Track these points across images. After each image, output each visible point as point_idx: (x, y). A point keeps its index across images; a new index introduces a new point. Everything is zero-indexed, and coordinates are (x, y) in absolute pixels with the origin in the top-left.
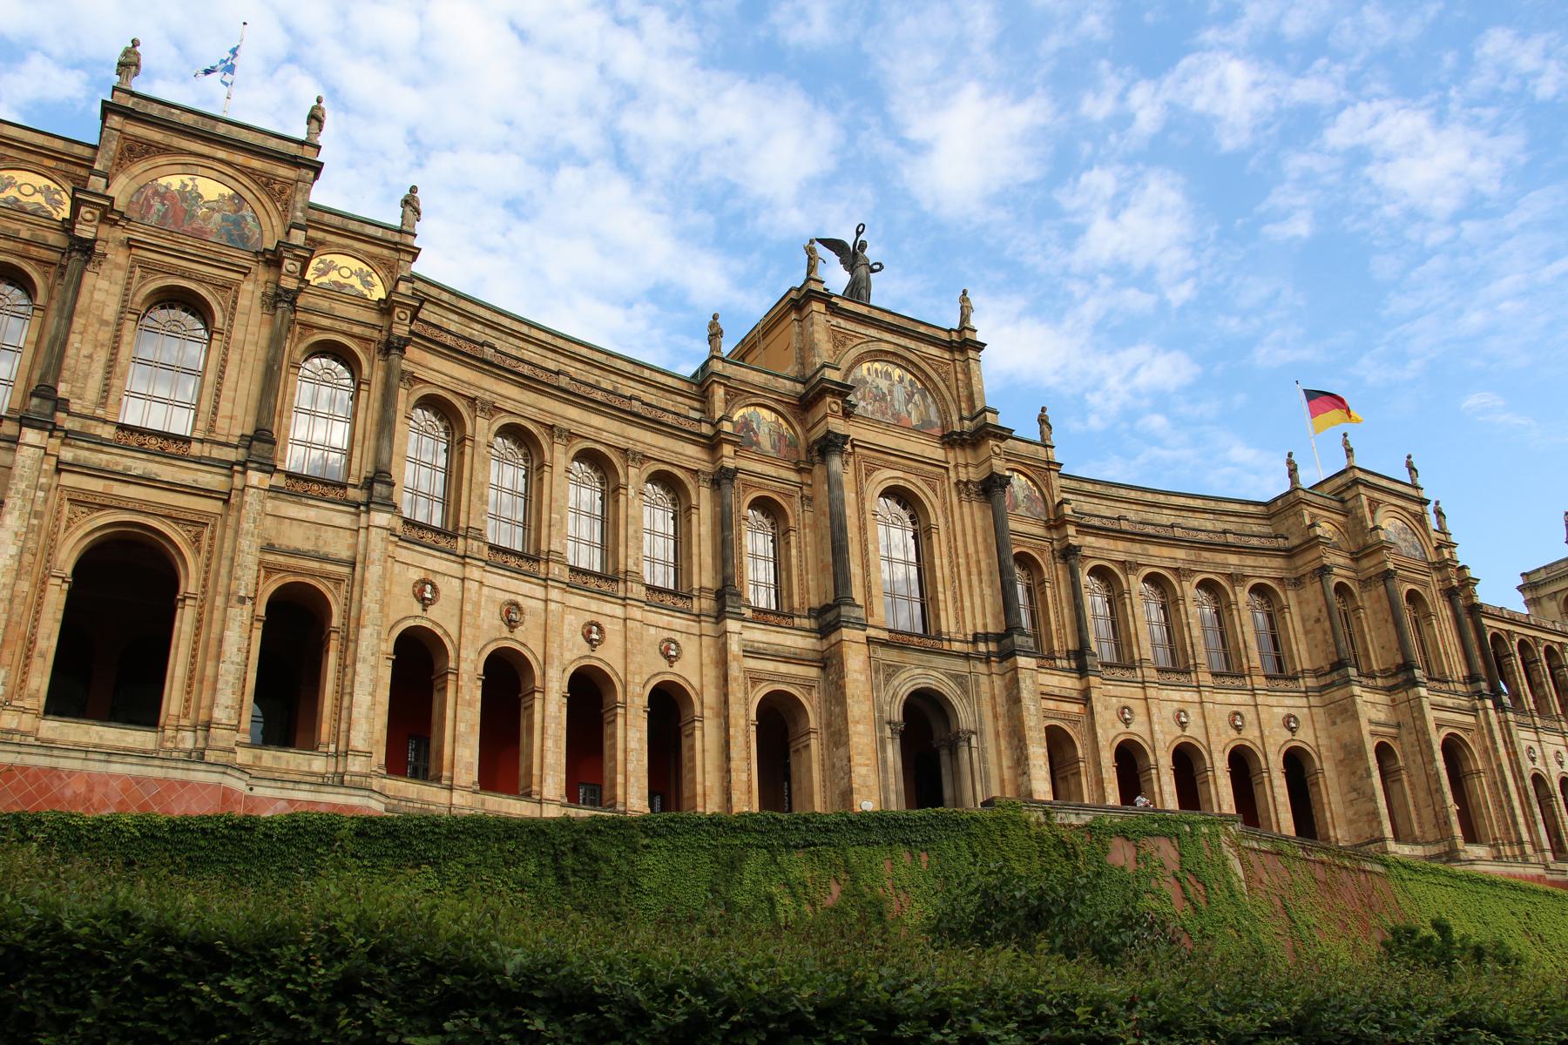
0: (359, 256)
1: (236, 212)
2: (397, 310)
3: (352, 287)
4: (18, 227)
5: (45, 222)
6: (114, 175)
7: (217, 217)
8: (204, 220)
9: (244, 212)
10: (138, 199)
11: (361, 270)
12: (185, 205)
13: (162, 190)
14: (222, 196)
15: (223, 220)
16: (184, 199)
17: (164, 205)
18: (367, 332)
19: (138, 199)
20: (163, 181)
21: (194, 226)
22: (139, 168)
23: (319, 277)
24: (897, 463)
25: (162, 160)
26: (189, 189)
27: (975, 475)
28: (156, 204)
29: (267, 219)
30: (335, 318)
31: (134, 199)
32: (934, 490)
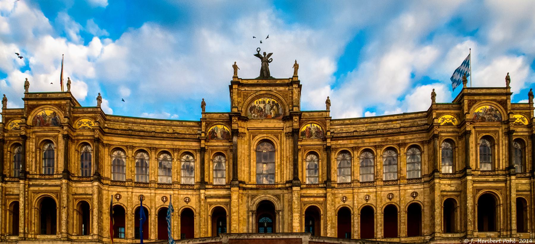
24: (264, 132)
27: (289, 130)
32: (277, 137)
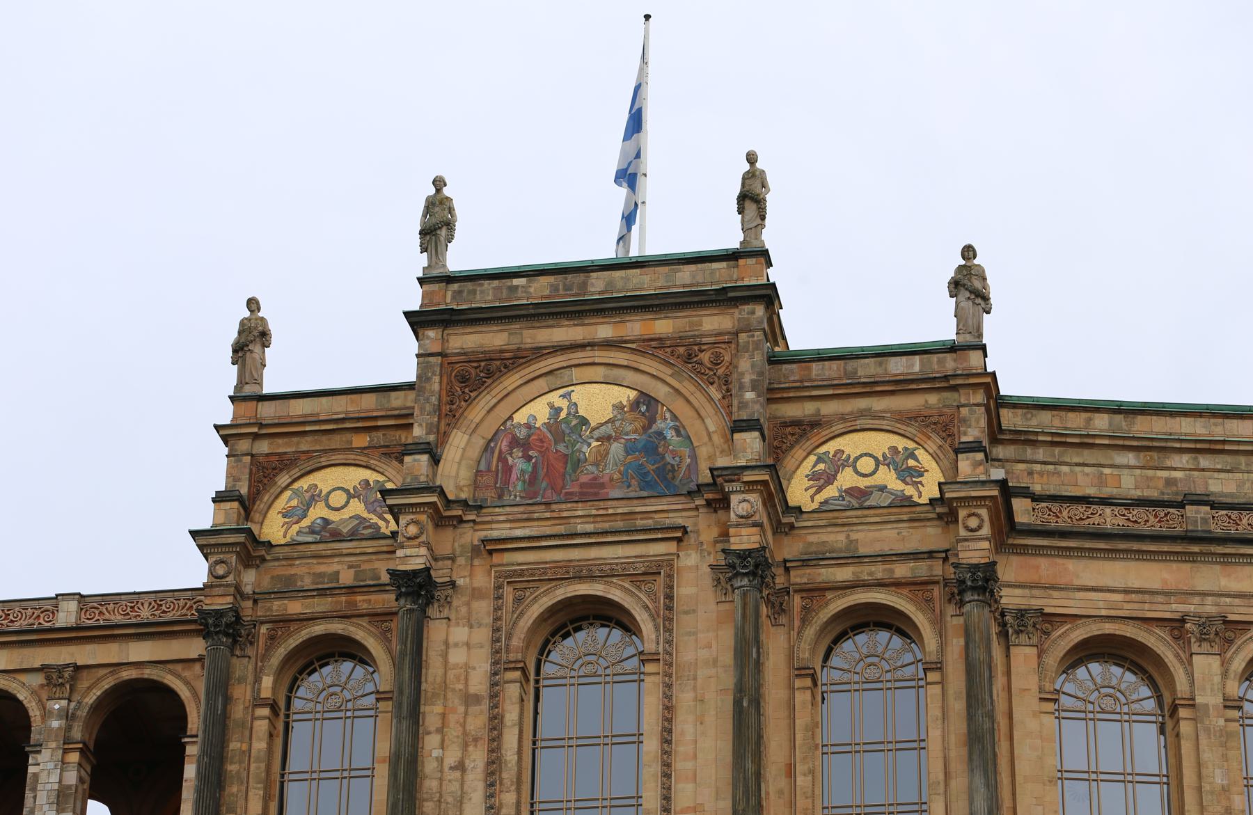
0: (885, 424)
1: (645, 428)
2: (962, 513)
3: (882, 489)
4: (336, 567)
5: (369, 546)
6: (443, 437)
7: (616, 448)
8: (597, 464)
9: (659, 424)
10: (489, 464)
11: (894, 450)
12: (561, 447)
13: (521, 434)
14: (619, 407)
15: (627, 453)
16: (559, 436)
17: (529, 458)
18: (921, 569)
19: (489, 464)
20: (521, 417)
21: (584, 479)
22: (476, 412)
23: (818, 492)
25: (512, 380)
26: (563, 415)
28: (518, 463)
29: (698, 422)
30: (859, 559)
31: (483, 467)
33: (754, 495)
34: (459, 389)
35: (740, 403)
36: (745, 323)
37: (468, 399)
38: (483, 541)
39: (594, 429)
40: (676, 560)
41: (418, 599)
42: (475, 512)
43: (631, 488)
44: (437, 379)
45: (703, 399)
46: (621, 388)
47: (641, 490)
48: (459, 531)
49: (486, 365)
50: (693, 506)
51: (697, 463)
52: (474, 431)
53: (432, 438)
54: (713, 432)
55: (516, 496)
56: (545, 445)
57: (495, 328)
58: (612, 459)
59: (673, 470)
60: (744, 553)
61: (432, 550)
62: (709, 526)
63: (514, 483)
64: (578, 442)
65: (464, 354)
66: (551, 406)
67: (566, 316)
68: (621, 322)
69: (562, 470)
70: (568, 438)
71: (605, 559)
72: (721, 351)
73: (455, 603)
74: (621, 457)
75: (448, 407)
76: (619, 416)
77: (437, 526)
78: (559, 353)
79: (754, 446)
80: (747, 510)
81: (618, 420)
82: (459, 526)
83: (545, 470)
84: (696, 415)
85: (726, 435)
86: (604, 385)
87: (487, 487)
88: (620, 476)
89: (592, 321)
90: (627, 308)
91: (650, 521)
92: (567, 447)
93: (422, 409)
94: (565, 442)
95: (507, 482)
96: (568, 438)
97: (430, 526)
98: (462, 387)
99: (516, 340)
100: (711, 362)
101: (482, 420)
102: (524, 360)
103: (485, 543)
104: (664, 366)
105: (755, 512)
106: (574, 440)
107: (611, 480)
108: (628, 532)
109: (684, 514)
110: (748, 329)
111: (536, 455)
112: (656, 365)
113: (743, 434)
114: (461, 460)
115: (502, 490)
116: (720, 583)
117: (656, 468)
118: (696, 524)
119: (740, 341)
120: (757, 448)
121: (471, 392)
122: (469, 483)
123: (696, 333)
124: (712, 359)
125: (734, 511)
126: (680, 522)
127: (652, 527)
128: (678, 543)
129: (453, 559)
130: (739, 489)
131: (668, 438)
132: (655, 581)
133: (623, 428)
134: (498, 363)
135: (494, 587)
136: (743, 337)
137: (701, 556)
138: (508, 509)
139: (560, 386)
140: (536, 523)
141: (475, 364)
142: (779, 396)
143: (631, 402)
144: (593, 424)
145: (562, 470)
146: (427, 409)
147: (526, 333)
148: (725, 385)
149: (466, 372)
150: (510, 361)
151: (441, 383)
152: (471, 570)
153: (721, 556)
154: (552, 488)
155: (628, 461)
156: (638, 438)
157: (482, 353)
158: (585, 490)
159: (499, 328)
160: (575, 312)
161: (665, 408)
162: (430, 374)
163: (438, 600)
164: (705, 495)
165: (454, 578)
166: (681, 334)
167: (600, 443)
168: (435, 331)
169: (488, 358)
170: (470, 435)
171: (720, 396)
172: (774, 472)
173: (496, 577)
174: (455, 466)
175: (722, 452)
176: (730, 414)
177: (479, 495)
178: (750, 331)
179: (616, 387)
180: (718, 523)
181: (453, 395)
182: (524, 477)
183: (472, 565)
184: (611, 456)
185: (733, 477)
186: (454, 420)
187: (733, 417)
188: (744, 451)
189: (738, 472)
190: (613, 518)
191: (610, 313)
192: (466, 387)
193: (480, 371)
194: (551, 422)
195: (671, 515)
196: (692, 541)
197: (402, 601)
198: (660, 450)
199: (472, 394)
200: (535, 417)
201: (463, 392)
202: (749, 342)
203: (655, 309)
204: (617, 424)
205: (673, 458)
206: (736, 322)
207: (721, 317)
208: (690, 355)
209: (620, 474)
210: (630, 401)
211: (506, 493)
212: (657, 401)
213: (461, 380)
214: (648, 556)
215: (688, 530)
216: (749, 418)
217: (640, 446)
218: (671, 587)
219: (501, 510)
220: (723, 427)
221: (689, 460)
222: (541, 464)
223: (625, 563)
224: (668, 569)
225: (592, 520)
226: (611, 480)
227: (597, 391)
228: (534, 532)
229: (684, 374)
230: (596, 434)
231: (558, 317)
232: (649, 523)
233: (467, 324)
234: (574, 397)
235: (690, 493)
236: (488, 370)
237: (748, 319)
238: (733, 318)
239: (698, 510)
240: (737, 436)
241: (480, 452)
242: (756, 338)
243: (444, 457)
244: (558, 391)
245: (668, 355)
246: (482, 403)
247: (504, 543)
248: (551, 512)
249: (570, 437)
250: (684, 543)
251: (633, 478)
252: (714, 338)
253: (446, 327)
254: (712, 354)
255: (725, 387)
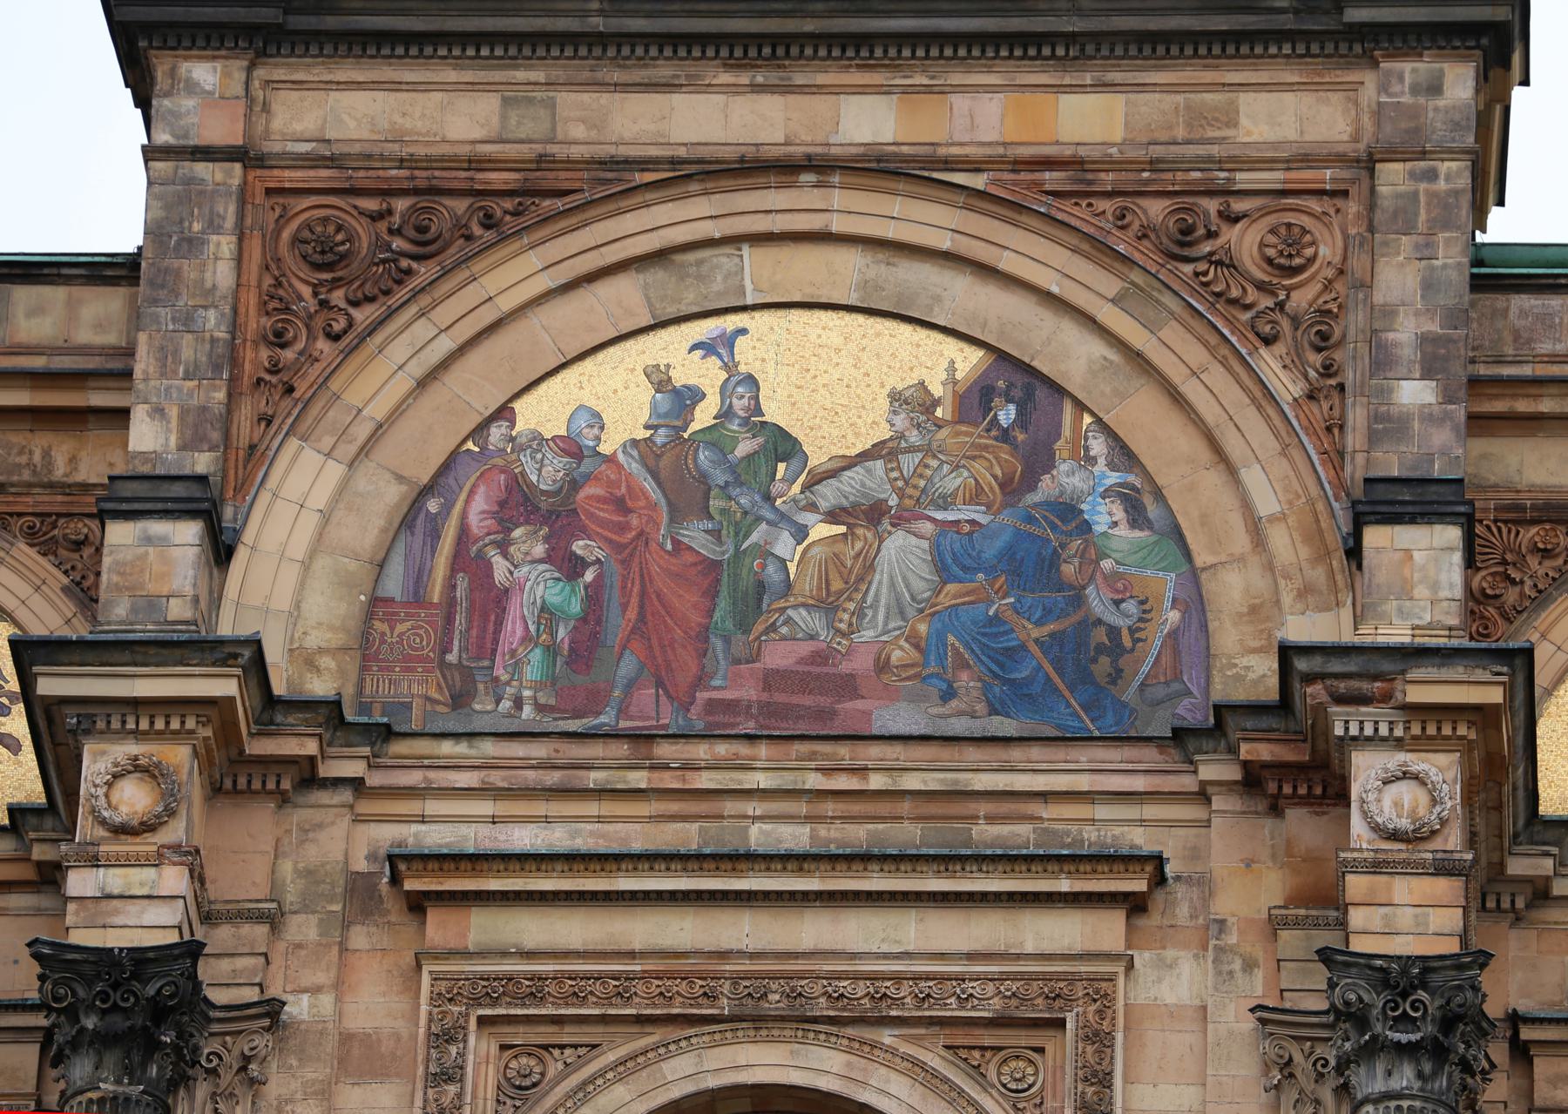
1: (1013, 488)
8: (827, 604)
9: (1065, 478)
10: (419, 579)
12: (695, 535)
13: (546, 473)
15: (944, 567)
17: (571, 567)
19: (419, 579)
21: (778, 656)
26: (704, 416)
29: (1213, 479)
31: (394, 585)
33: (1442, 759)
34: (306, 291)
35: (1376, 418)
36: (1404, 125)
37: (345, 332)
38: (391, 858)
39: (817, 479)
40: (1121, 980)
41: (144, 1065)
42: (366, 751)
43: (954, 703)
44: (224, 245)
45: (1233, 395)
46: (922, 333)
47: (993, 711)
48: (298, 816)
49: (414, 209)
50: (1187, 783)
51: (1204, 627)
52: (365, 450)
53: (203, 462)
54: (1272, 519)
55: (518, 703)
56: (635, 521)
57: (452, 75)
58: (884, 590)
59: (1114, 647)
60: (1404, 972)
61: (202, 881)
62: (1249, 863)
63: (513, 653)
64: (759, 519)
65: (332, 161)
66: (660, 380)
67: (724, 52)
68: (928, 90)
69: (696, 618)
70: (721, 504)
71: (854, 956)
72: (1305, 221)
73: (276, 1087)
74: (918, 585)
75: (264, 354)
76: (914, 437)
77: (216, 791)
78: (694, 187)
79: (1443, 577)
80: (1414, 811)
81: (911, 450)
82: (300, 800)
83: (632, 614)
84: (1204, 454)
85: (1320, 531)
86: (860, 319)
87: (409, 662)
88: (914, 655)
89: (821, 79)
90: (956, 39)
91: (1024, 830)
92: (716, 534)
93: (166, 357)
94: (711, 518)
95: (486, 647)
96: (721, 504)
97: (195, 790)
98: (321, 283)
99: (529, 125)
100: (1270, 261)
101: (397, 412)
102: (559, 204)
103: (402, 867)
104: (1091, 266)
105: (1444, 822)
106: (746, 513)
107: (882, 666)
108: (946, 861)
109: (1151, 811)
110: (1414, 150)
111: (600, 554)
112: (1060, 256)
113: (1398, 529)
114: (313, 553)
115: (468, 674)
116: (1291, 1075)
117: (1052, 635)
118: (1195, 854)
119: (1383, 190)
120: (1451, 586)
121: (355, 304)
122: (335, 639)
123: (1215, 150)
124: (1271, 252)
125: (1365, 814)
126: (1139, 841)
127: (1032, 850)
128: (1128, 917)
129: (274, 920)
130: (1384, 730)
131: (1099, 529)
132: (1040, 1050)
133: (930, 480)
134: (460, 205)
135: (429, 1034)
136: (1393, 177)
137: (1219, 973)
138: (489, 748)
139: (695, 309)
140: (592, 808)
141: (371, 204)
142: (1499, 406)
143: (961, 389)
144: (817, 459)
145: (696, 618)
146: (187, 353)
147: (570, 102)
148: (1319, 350)
149: (339, 228)
150: (508, 204)
151: (239, 259)
152: (342, 965)
153: (1319, 976)
154: (660, 684)
155: (945, 600)
156: (983, 519)
157: (402, 162)
158: (780, 698)
159: (468, 76)
160: (759, 39)
161: (1087, 419)
162: (197, 227)
163: (213, 1072)
164: (1244, 748)
165: (274, 991)
166: (1158, 151)
167: (842, 529)
168: (218, 65)
169: (422, 184)
170: (351, 465)
171: (1298, 389)
172: (1520, 679)
173: (436, 998)
174: (290, 574)
175: (1305, 592)
176: (1336, 458)
177: (381, 688)
178: (1423, 155)
179: (905, 330)
180: (1287, 854)
181: (287, 310)
182: (553, 634)
183: (343, 949)
184: (880, 578)
185: (1365, 686)
186: (287, 403)
187: (1348, 469)
188: (1406, 593)
189: (1386, 666)
190: (883, 808)
191: (892, 52)
192: (335, 283)
193: (391, 231)
194: (659, 440)
195: (1102, 811)
196: (1183, 911)
197: (81, 1069)
198: (1068, 570)
199: (359, 315)
200: (598, 416)
201: (324, 304)
202: (1416, 194)
203: (1060, 52)
204: (909, 462)
205: (1117, 603)
206: (1367, 121)
207: (1307, 99)
208: (1187, 230)
209: (917, 646)
210: (955, 383)
211: (481, 687)
212: (1059, 390)
213: (318, 258)
214: (1018, 957)
215: (1169, 870)
216: (1406, 474)
217: (991, 550)
218: (1104, 1080)
219: (462, 748)
220: (1311, 502)
221: (1174, 616)
222: (616, 593)
223: (928, 977)
224: (1093, 1008)
225: (802, 808)
226: (882, 666)
227: (837, 340)
228: (584, 839)
229: (1168, 300)
230: (828, 495)
231: (696, 53)
232: (1019, 835)
233: (343, 49)
234: (747, 354)
235: (1180, 735)
236: (422, 230)
237: (1414, 113)
238: (1356, 104)
239: (1209, 801)
240: (1374, 537)
241: (384, 530)
242: (1442, 185)
243: (248, 536)
244: (686, 328)
245: (1108, 226)
246: (399, 350)
247: (476, 873)
248: (652, 768)
249: (730, 498)
250: (1153, 920)
251: (968, 666)
252: (1279, 175)
253: (262, 54)
254: (1273, 231)
255: (1316, 359)
